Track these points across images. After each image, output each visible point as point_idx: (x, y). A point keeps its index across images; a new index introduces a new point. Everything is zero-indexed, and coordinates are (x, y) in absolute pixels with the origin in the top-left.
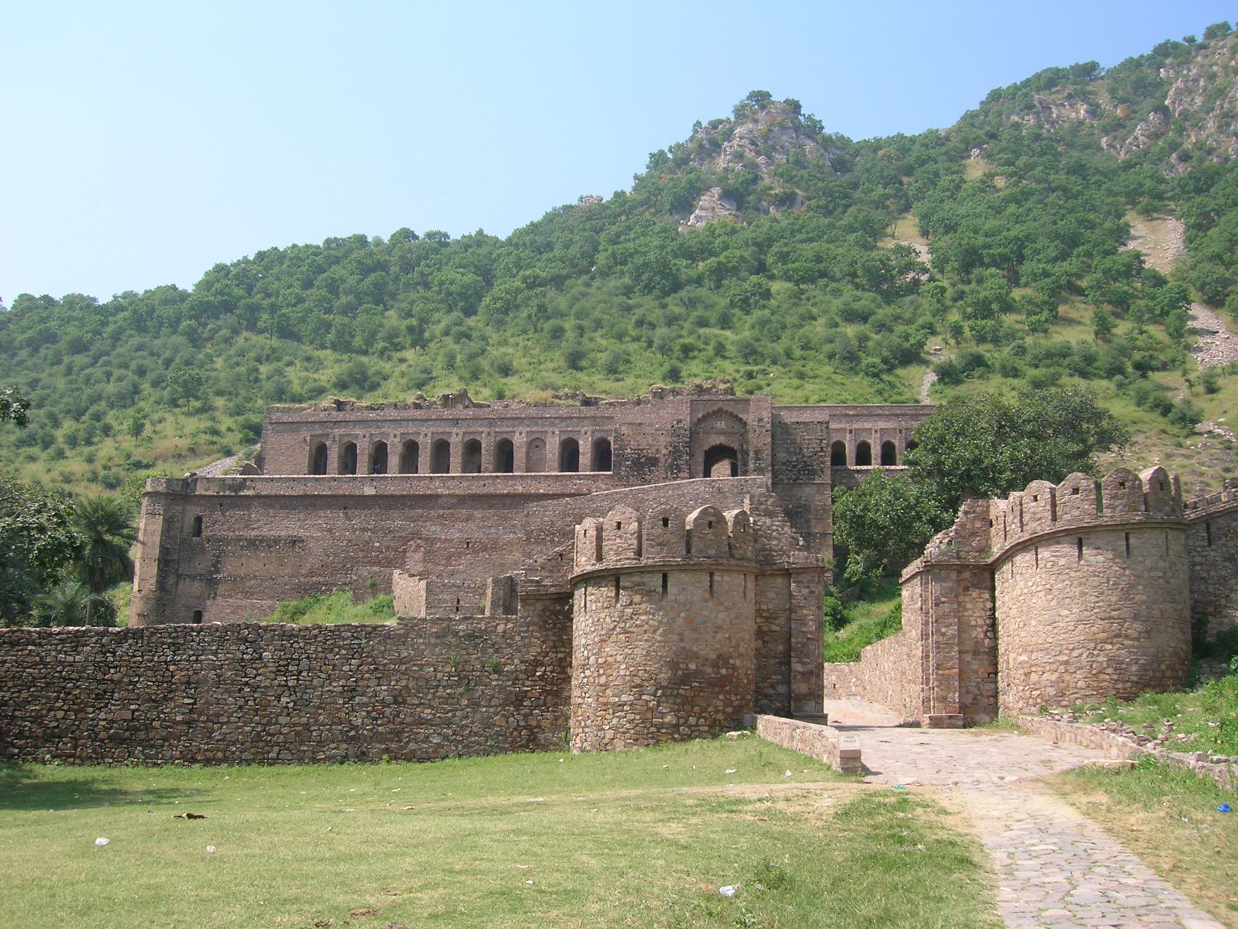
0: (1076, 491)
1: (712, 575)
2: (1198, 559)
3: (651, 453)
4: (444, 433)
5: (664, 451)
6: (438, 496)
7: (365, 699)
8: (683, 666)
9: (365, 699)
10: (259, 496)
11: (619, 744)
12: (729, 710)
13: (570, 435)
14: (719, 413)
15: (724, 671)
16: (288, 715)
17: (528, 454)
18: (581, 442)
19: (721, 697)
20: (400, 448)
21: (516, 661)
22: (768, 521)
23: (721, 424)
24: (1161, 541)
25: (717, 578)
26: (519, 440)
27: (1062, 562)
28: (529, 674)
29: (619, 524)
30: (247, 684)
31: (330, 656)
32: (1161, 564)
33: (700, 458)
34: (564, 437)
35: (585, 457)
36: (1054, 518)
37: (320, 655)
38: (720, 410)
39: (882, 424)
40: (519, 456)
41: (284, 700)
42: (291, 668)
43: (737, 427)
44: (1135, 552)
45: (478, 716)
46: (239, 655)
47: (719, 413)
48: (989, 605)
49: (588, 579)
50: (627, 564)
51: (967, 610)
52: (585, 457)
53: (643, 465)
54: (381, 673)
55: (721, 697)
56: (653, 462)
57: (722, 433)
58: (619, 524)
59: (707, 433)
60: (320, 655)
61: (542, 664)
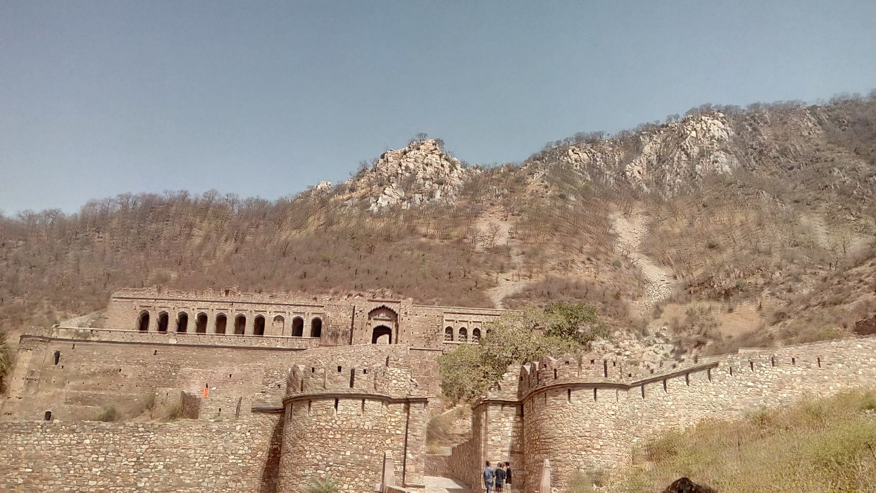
0: (567, 362)
1: (364, 401)
2: (636, 406)
7: (148, 470)
8: (342, 453)
9: (148, 470)
12: (368, 480)
15: (366, 457)
16: (96, 479)
19: (363, 472)
20: (196, 318)
21: (246, 448)
22: (399, 371)
23: (382, 315)
24: (614, 394)
25: (366, 402)
26: (269, 317)
27: (559, 402)
29: (313, 369)
30: (71, 459)
31: (129, 443)
32: (614, 407)
35: (307, 329)
37: (123, 442)
38: (383, 306)
41: (94, 470)
42: (102, 450)
44: (599, 399)
45: (218, 481)
46: (68, 440)
50: (316, 392)
51: (506, 427)
52: (307, 329)
55: (363, 472)
58: (313, 369)
60: (123, 442)
61: (261, 450)
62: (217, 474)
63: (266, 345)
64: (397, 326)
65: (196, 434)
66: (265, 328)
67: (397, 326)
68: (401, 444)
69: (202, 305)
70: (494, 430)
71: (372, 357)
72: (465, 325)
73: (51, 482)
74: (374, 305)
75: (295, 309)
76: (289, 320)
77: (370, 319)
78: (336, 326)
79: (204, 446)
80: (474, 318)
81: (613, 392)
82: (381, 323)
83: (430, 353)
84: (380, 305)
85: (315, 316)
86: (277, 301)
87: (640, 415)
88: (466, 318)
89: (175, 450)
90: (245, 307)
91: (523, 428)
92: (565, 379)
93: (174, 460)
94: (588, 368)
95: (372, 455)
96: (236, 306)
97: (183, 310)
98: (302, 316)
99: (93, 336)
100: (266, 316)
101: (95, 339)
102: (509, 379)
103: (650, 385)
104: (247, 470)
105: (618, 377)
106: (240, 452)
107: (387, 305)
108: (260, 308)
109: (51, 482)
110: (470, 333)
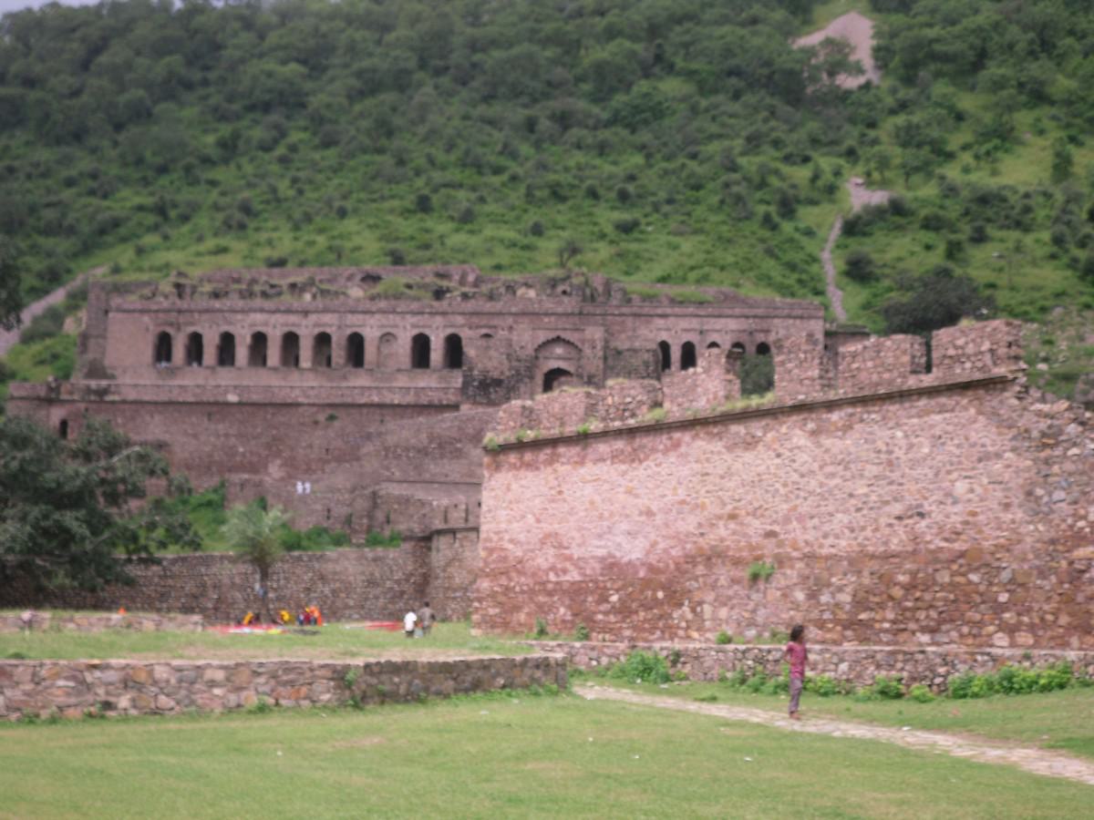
3: (495, 374)
4: (293, 325)
5: (507, 373)
6: (299, 405)
10: (124, 402)
11: (454, 618)
14: (558, 340)
17: (379, 348)
20: (248, 340)
23: (559, 350)
26: (371, 334)
28: (407, 580)
33: (539, 380)
34: (416, 332)
35: (437, 355)
39: (733, 324)
40: (370, 353)
43: (573, 353)
47: (558, 340)
49: (440, 532)
52: (437, 355)
53: (488, 386)
54: (322, 578)
56: (498, 383)
57: (559, 358)
59: (546, 358)
62: (377, 598)
63: (376, 399)
69: (259, 317)
74: (543, 336)
75: (414, 320)
84: (552, 335)
85: (449, 331)
96: (313, 318)
98: (427, 332)
99: (114, 393)
101: (116, 398)
104: (402, 593)
107: (564, 335)
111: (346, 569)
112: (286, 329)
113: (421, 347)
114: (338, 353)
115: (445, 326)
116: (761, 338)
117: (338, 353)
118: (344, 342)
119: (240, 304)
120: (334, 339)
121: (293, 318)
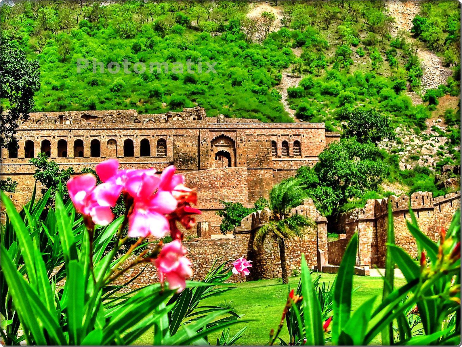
13: (129, 138)
18: (134, 141)
21: (236, 253)
23: (222, 142)
26: (103, 140)
27: (399, 220)
35: (137, 150)
36: (397, 207)
48: (375, 231)
52: (137, 150)
53: (187, 161)
61: (244, 253)
64: (235, 151)
65: (210, 247)
66: (101, 151)
67: (235, 151)
68: (315, 246)
69: (45, 133)
70: (363, 235)
71: (221, 178)
72: (274, 139)
73: (144, 275)
74: (215, 135)
75: (125, 132)
76: (121, 142)
77: (212, 146)
78: (185, 154)
79: (215, 253)
80: (282, 132)
81: (427, 212)
82: (220, 149)
83: (262, 171)
84: (219, 134)
85: (143, 138)
86: (109, 125)
87: (438, 221)
88: (275, 132)
89: (201, 256)
90: (81, 133)
91: (377, 233)
92: (403, 208)
93: (201, 261)
94: (415, 201)
95: (309, 253)
97: (29, 138)
98: (132, 138)
100: (101, 139)
102: (369, 207)
103: (444, 205)
105: (429, 204)
106: (234, 255)
107: (225, 134)
108: (94, 133)
109: (144, 275)
110: (279, 145)
111: (206, 251)
112: (60, 138)
113: (129, 147)
114: (87, 150)
115: (141, 136)
116: (296, 138)
117: (87, 150)
118: (90, 145)
119: (36, 126)
120: (84, 143)
121: (62, 133)
